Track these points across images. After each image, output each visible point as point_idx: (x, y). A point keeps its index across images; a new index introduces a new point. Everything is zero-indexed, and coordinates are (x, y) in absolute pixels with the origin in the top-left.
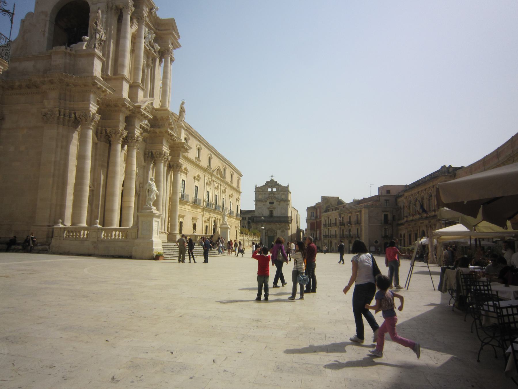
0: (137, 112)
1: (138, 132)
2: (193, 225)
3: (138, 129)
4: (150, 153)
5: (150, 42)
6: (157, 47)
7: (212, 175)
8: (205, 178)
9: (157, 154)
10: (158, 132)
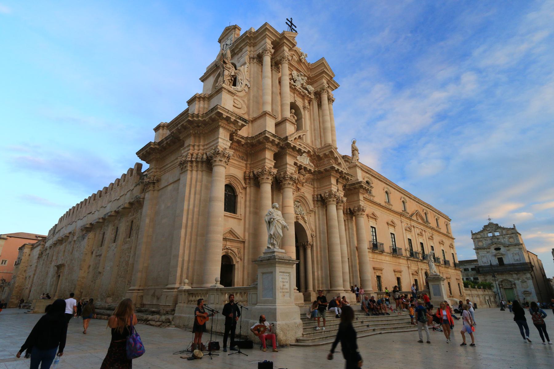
1: (292, 170)
2: (396, 280)
3: (290, 165)
4: (319, 196)
5: (302, 84)
6: (311, 88)
7: (410, 219)
8: (401, 224)
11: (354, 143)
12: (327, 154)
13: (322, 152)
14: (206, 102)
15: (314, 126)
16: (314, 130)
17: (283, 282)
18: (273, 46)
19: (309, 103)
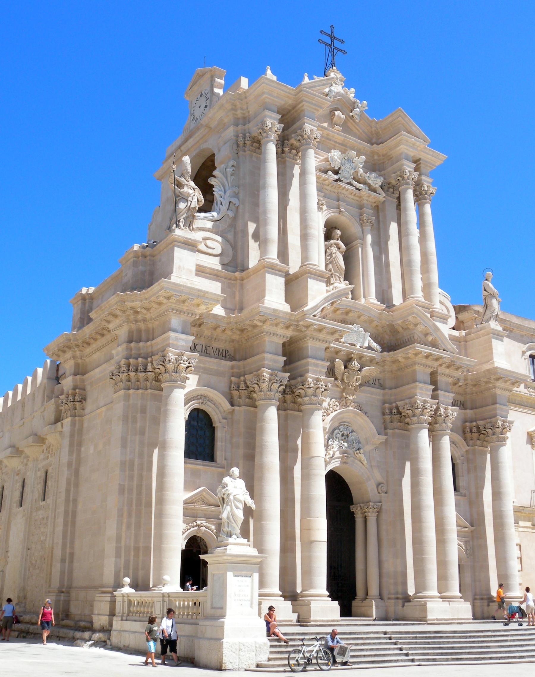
0: (304, 326)
4: (394, 411)
9: (406, 409)
10: (400, 359)
17: (239, 586)
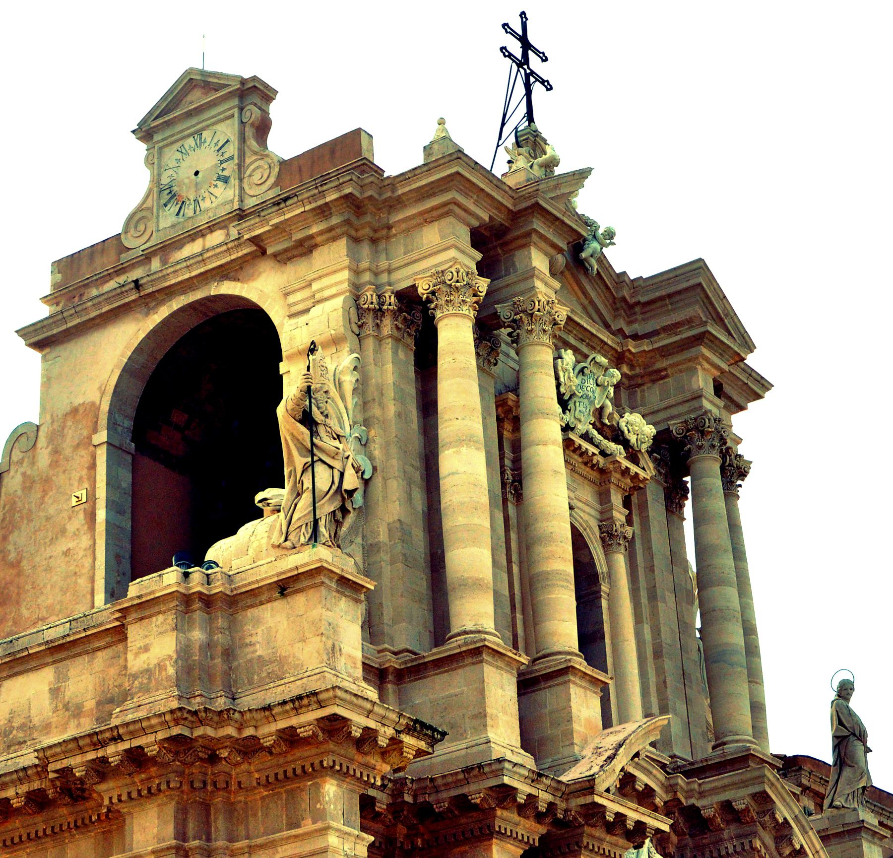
11: (845, 690)
12: (739, 806)
13: (714, 791)
14: (220, 622)
15: (656, 632)
16: (658, 654)
18: (479, 256)
19: (627, 503)
